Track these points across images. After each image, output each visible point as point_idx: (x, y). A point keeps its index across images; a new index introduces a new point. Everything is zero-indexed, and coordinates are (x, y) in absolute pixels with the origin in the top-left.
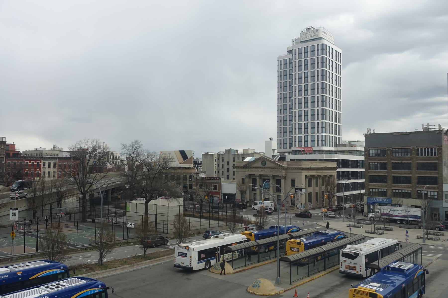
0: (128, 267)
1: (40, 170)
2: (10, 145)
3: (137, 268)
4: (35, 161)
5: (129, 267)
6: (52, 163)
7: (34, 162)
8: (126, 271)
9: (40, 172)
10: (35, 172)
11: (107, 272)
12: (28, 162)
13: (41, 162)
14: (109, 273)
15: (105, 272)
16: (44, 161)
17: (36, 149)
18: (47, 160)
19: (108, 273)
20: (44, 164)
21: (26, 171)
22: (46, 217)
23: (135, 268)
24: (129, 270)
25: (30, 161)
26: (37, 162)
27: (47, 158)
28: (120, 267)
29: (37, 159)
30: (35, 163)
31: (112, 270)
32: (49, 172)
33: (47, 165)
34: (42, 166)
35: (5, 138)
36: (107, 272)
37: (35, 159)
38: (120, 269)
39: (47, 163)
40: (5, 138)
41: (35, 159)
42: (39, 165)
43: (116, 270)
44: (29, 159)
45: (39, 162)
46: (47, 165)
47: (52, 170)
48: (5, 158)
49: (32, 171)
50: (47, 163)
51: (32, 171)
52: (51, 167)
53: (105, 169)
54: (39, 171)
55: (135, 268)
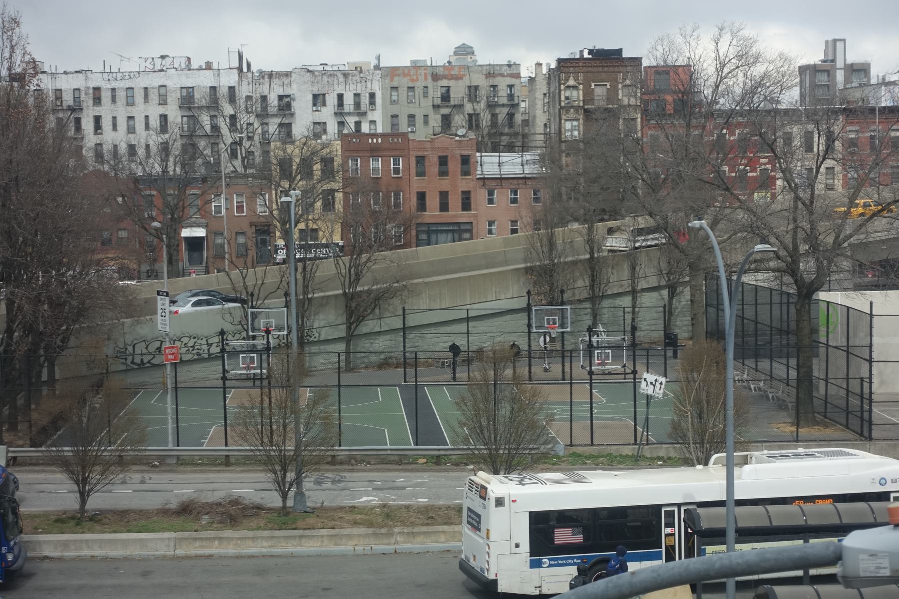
0: (359, 535)
3: (402, 546)
5: (366, 535)
8: (347, 547)
10: (753, 170)
11: (262, 538)
14: (270, 543)
15: (254, 538)
17: (883, 79)
19: (265, 544)
22: (542, 339)
23: (393, 546)
24: (359, 548)
28: (324, 532)
31: (286, 537)
35: (844, 41)
36: (262, 538)
38: (322, 536)
40: (844, 41)
43: (301, 537)
48: (639, 120)
54: (769, 167)
55: (393, 546)
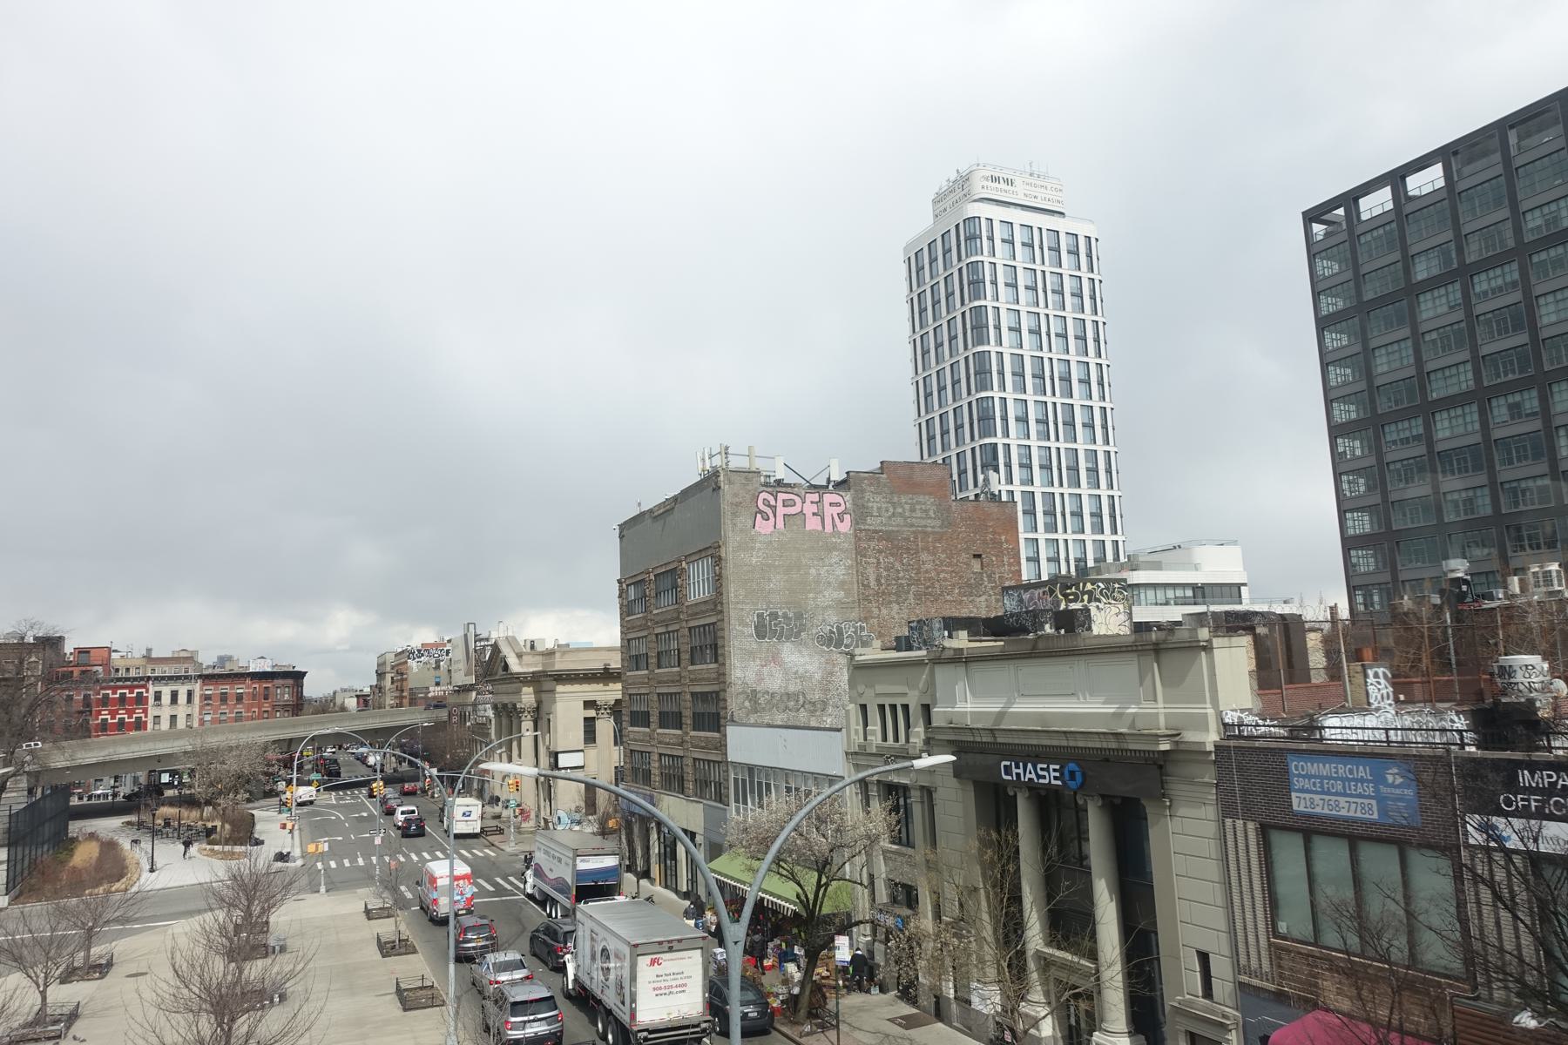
1: (145, 711)
2: (92, 651)
4: (131, 689)
6: (182, 691)
7: (126, 691)
9: (146, 717)
12: (110, 692)
13: (147, 691)
16: (157, 689)
18: (166, 684)
20: (158, 696)
21: (101, 717)
25: (114, 689)
26: (136, 691)
27: (163, 678)
29: (136, 683)
30: (128, 695)
32: (173, 718)
33: (166, 699)
34: (151, 701)
37: (129, 683)
39: (166, 691)
41: (129, 683)
42: (140, 700)
44: (112, 684)
45: (144, 690)
46: (166, 699)
47: (181, 710)
49: (105, 715)
50: (166, 691)
51: (122, 714)
52: (179, 702)
53: (421, 698)
54: (143, 715)
